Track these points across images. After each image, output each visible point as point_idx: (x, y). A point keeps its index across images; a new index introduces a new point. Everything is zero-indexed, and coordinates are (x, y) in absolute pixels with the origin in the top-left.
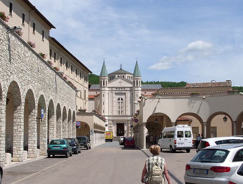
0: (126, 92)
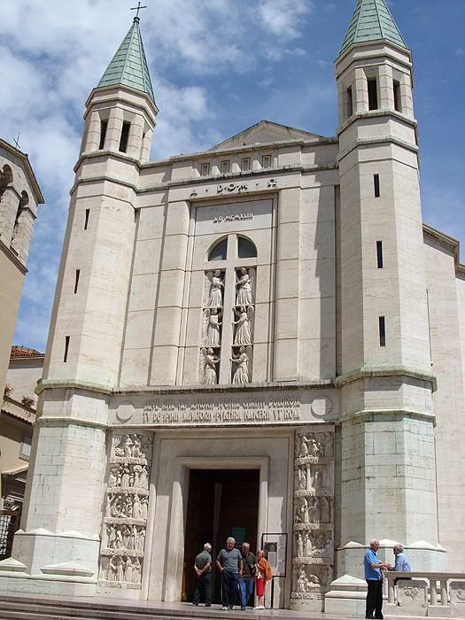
0: (281, 181)
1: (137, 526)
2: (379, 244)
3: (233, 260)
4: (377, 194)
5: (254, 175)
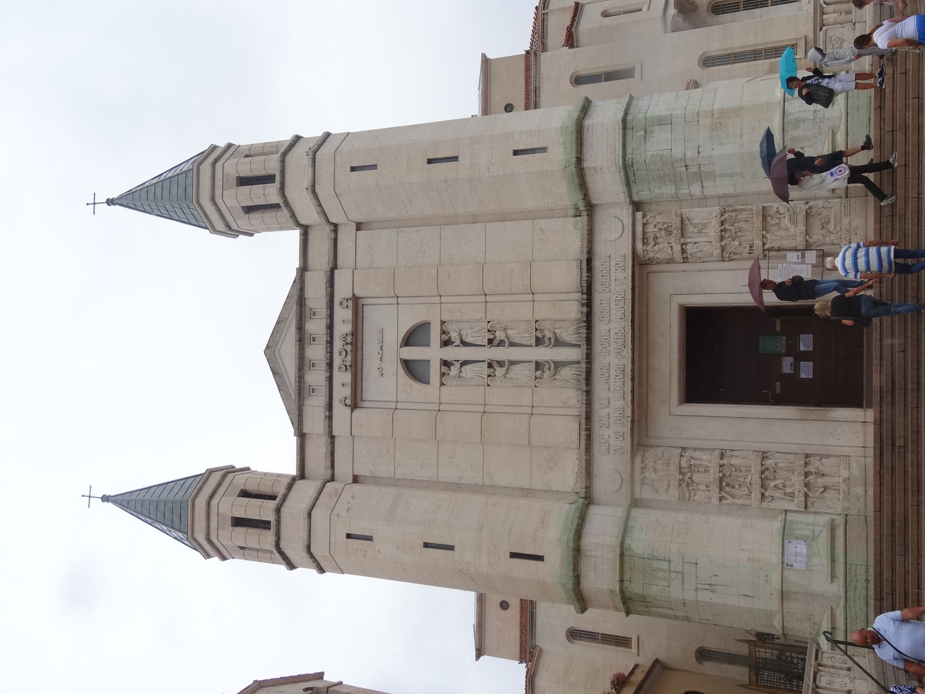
0: (342, 291)
1: (763, 460)
2: (430, 161)
3: (432, 353)
4: (374, 167)
5: (330, 327)
